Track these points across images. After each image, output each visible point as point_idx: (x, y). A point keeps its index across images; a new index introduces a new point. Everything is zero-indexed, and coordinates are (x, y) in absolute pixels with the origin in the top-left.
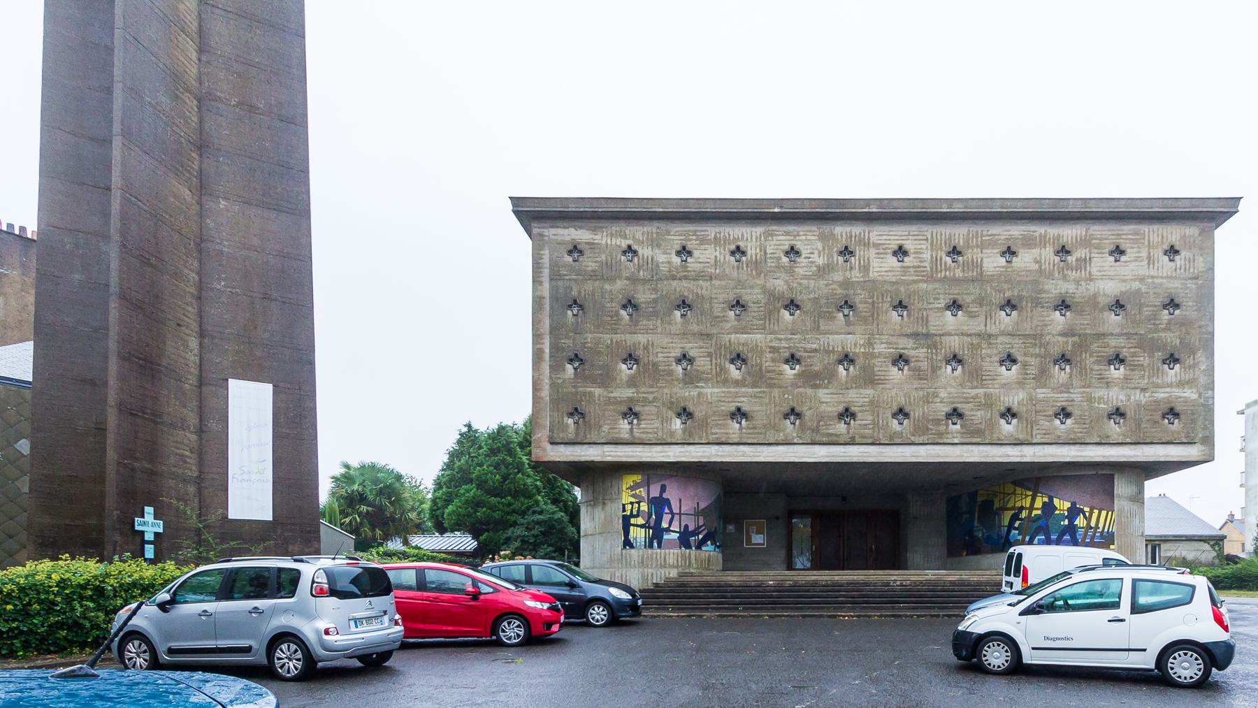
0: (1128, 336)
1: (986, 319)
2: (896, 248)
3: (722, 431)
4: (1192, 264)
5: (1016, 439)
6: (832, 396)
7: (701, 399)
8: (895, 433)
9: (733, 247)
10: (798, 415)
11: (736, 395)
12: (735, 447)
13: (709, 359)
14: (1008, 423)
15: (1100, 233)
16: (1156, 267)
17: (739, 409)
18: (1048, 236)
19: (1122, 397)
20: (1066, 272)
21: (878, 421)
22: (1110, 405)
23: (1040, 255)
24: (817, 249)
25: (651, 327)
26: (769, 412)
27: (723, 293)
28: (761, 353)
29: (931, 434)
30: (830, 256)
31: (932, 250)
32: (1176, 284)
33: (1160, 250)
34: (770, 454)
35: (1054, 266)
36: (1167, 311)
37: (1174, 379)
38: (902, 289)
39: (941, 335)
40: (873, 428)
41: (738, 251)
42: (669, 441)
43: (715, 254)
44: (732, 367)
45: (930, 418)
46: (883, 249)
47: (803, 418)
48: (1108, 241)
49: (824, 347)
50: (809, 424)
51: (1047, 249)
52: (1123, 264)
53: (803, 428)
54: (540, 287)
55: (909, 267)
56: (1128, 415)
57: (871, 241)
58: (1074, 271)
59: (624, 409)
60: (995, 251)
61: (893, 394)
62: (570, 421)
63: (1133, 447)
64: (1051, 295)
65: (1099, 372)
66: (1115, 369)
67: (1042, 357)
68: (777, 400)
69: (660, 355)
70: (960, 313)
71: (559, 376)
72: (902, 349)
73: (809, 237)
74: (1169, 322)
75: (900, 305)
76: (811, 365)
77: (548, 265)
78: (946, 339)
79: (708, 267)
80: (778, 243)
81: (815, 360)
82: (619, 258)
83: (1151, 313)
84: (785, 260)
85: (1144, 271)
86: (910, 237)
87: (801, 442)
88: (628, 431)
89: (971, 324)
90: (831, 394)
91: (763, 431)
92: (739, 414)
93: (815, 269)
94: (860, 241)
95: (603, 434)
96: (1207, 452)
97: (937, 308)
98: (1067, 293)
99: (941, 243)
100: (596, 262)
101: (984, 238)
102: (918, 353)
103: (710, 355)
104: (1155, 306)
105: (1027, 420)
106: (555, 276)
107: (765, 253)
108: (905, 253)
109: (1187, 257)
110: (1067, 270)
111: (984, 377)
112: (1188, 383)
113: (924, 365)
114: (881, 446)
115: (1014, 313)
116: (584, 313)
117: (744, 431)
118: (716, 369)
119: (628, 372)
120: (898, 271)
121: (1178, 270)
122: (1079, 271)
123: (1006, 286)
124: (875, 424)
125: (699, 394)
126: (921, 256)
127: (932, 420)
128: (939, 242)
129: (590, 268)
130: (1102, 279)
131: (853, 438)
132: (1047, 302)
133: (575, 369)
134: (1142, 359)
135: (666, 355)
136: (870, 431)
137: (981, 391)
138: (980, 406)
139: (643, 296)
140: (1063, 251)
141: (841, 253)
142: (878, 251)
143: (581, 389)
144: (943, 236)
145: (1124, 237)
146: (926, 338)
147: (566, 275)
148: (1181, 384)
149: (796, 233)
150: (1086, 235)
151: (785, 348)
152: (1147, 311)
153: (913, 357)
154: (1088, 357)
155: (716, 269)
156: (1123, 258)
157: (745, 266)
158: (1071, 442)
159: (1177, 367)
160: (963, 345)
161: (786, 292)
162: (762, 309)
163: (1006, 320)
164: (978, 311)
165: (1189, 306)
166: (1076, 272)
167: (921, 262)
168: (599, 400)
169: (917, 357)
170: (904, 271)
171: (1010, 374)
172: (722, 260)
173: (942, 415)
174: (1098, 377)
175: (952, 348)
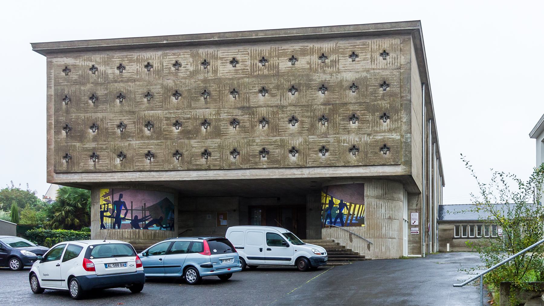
0: (360, 104)
1: (281, 98)
2: (231, 59)
4: (396, 60)
5: (298, 165)
6: (198, 143)
7: (130, 147)
8: (232, 163)
9: (146, 63)
10: (181, 155)
11: (148, 145)
12: (149, 173)
13: (134, 125)
14: (294, 156)
15: (343, 45)
16: (375, 64)
17: (149, 152)
18: (315, 49)
19: (357, 139)
20: (325, 69)
21: (223, 156)
22: (350, 144)
23: (310, 59)
24: (190, 62)
25: (104, 109)
26: (165, 153)
27: (141, 89)
28: (161, 121)
29: (252, 163)
30: (197, 65)
31: (251, 60)
32: (387, 73)
33: (378, 53)
35: (318, 65)
36: (382, 89)
37: (386, 128)
38: (235, 82)
39: (256, 107)
40: (220, 161)
41: (148, 66)
42: (114, 170)
43: (137, 67)
44: (146, 129)
45: (251, 154)
46: (225, 60)
47: (183, 156)
48: (348, 50)
49: (194, 116)
50: (186, 159)
51: (314, 56)
52: (357, 62)
53: (183, 162)
54: (50, 90)
55: (239, 70)
56: (360, 150)
57: (218, 56)
58: (329, 68)
59: (91, 153)
60: (286, 58)
61: (231, 141)
62: (64, 161)
63: (364, 168)
64: (316, 82)
65: (344, 125)
66: (353, 123)
67: (311, 118)
68: (170, 147)
69: (109, 124)
70: (266, 94)
71: (58, 137)
72: (235, 116)
73: (185, 56)
74: (383, 95)
75: (233, 92)
76: (187, 127)
77: (53, 78)
78: (259, 110)
79: (133, 75)
80: (170, 60)
81: (189, 124)
82: (88, 72)
83: (372, 90)
84: (173, 69)
85: (369, 66)
86: (239, 53)
87: (182, 169)
88: (93, 165)
89: (273, 100)
90: (198, 142)
92: (149, 154)
93: (189, 73)
94: (212, 56)
95: (80, 167)
96: (408, 170)
97: (254, 92)
98: (326, 80)
99: (256, 56)
100: (77, 75)
101: (279, 51)
102: (244, 118)
103: (134, 123)
104: (375, 86)
105: (304, 154)
106: (57, 84)
107: (163, 66)
108: (237, 62)
109: (394, 57)
110: (325, 67)
111: (280, 130)
112: (394, 130)
113: (247, 124)
115: (296, 93)
116: (71, 102)
117: (152, 164)
118: (138, 130)
119: (93, 133)
120: (233, 72)
121: (388, 65)
122: (332, 67)
123: (291, 78)
124: (221, 158)
125: (129, 145)
126: (245, 63)
127: (252, 155)
128: (255, 55)
129: (74, 79)
130: (345, 72)
131: (209, 166)
132: (315, 86)
133: (67, 133)
134: (368, 117)
135: (112, 124)
137: (278, 138)
138: (278, 146)
139: (100, 92)
140: (323, 56)
141: (203, 64)
142: (222, 62)
143: (69, 144)
144: (257, 51)
145: (357, 47)
146: (248, 110)
147: (62, 83)
148: (390, 131)
149: (178, 54)
150: (336, 47)
151: (173, 117)
152: (370, 89)
153: (241, 120)
154: (337, 117)
155: (137, 76)
156: (357, 59)
157: (152, 73)
158: (328, 166)
159: (388, 121)
160: (269, 113)
161: (174, 87)
162: (161, 97)
163: (292, 97)
164: (276, 93)
165: (395, 85)
166: (331, 69)
167: (245, 66)
168: (79, 149)
169: (243, 120)
170: (236, 72)
171: (294, 128)
172: (140, 70)
173: (257, 152)
174: (343, 128)
175: (263, 115)
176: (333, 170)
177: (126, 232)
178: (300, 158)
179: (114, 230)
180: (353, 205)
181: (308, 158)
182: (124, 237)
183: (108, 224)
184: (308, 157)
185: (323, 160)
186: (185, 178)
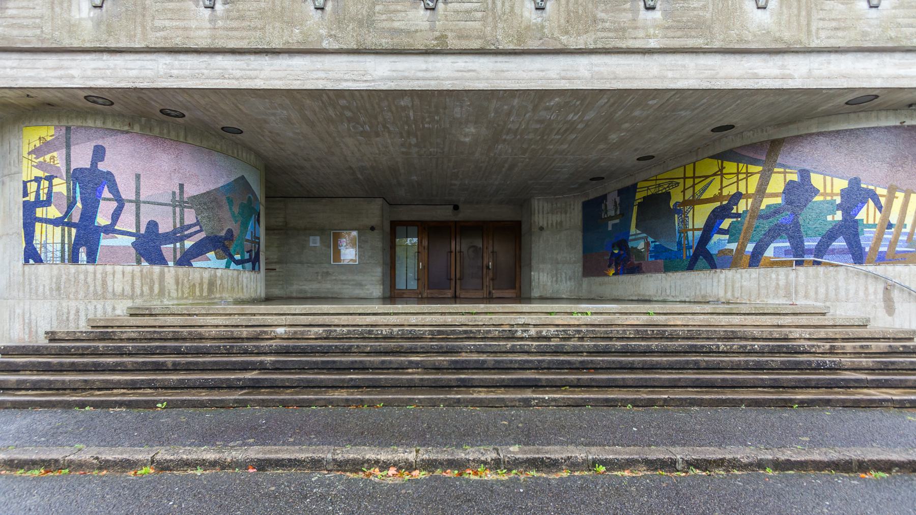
3: (174, 23)
8: (528, 28)
12: (205, 58)
29: (604, 30)
34: (274, 74)
40: (484, 19)
87: (336, 46)
91: (259, 23)
114: (500, 59)
117: (220, 23)
131: (442, 38)
136: (477, 25)
176: (895, 65)
177: (119, 276)
178: (785, 17)
179: (72, 268)
180: (900, 196)
181: (815, 15)
182: (110, 289)
183: (50, 248)
184: (814, 12)
185: (870, 26)
186: (346, 80)
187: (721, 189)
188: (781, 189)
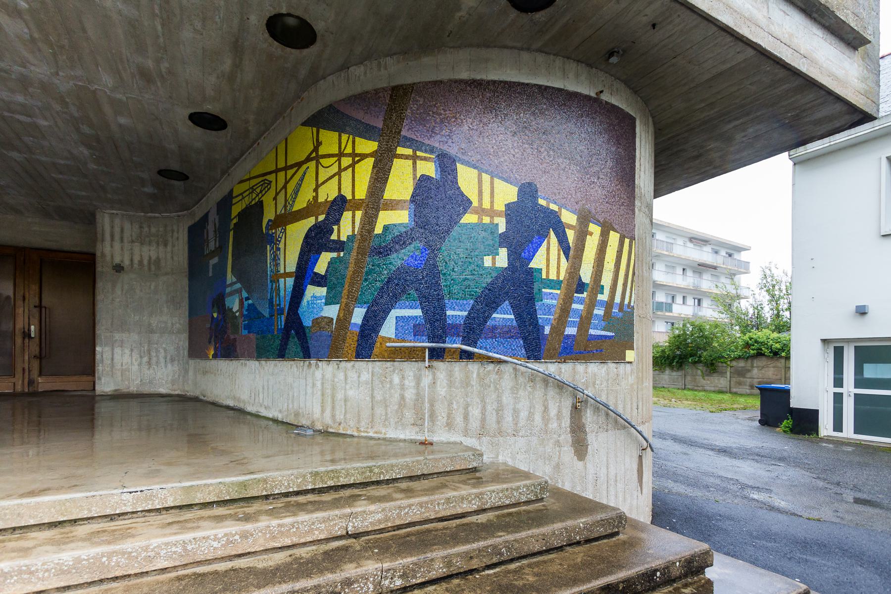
187: (316, 190)
188: (407, 195)
